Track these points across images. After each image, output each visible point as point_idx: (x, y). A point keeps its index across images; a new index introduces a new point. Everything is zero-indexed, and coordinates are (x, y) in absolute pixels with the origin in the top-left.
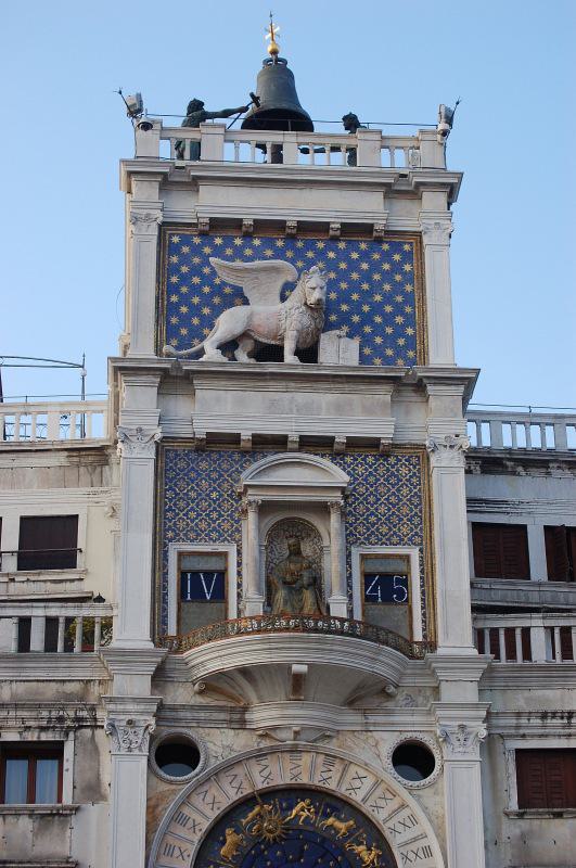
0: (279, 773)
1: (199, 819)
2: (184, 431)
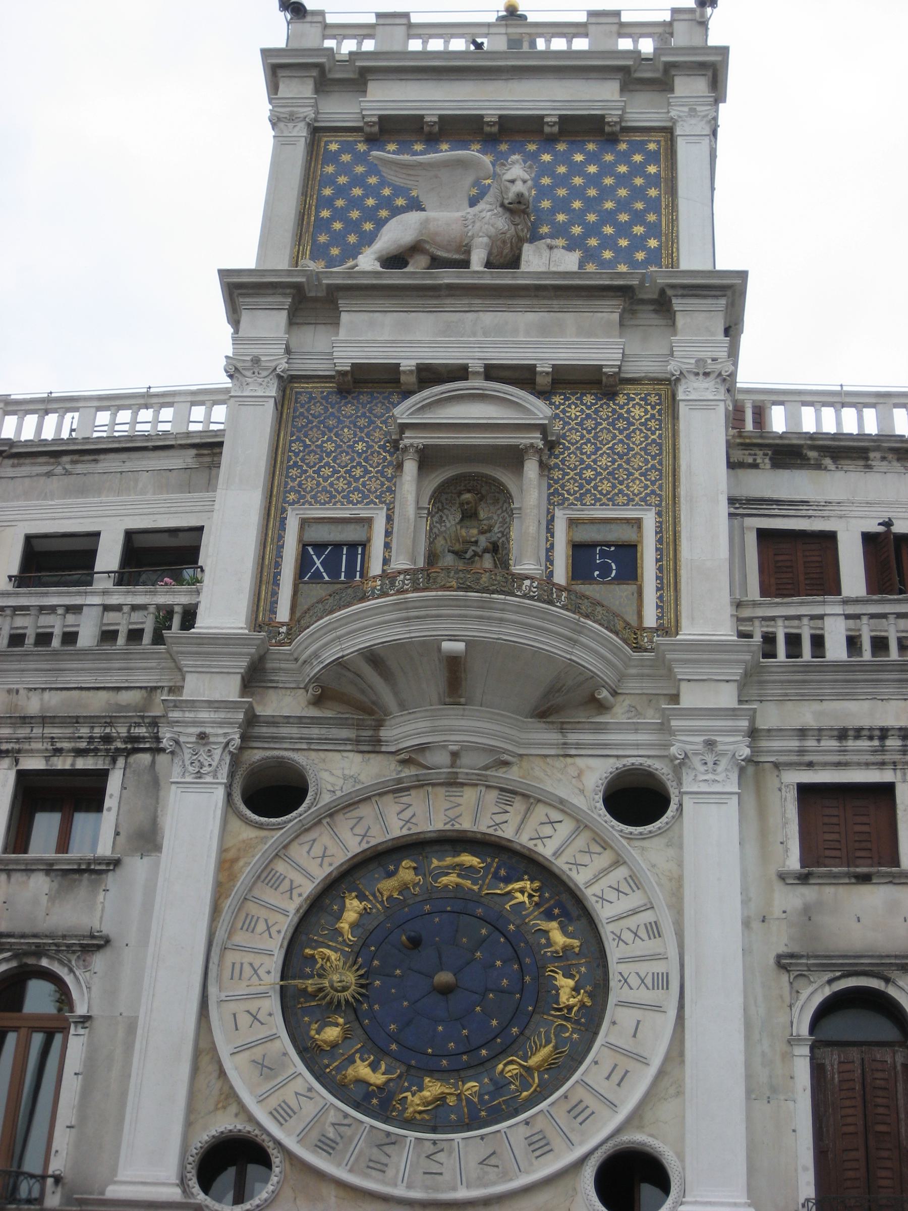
0: (430, 815)
1: (298, 879)
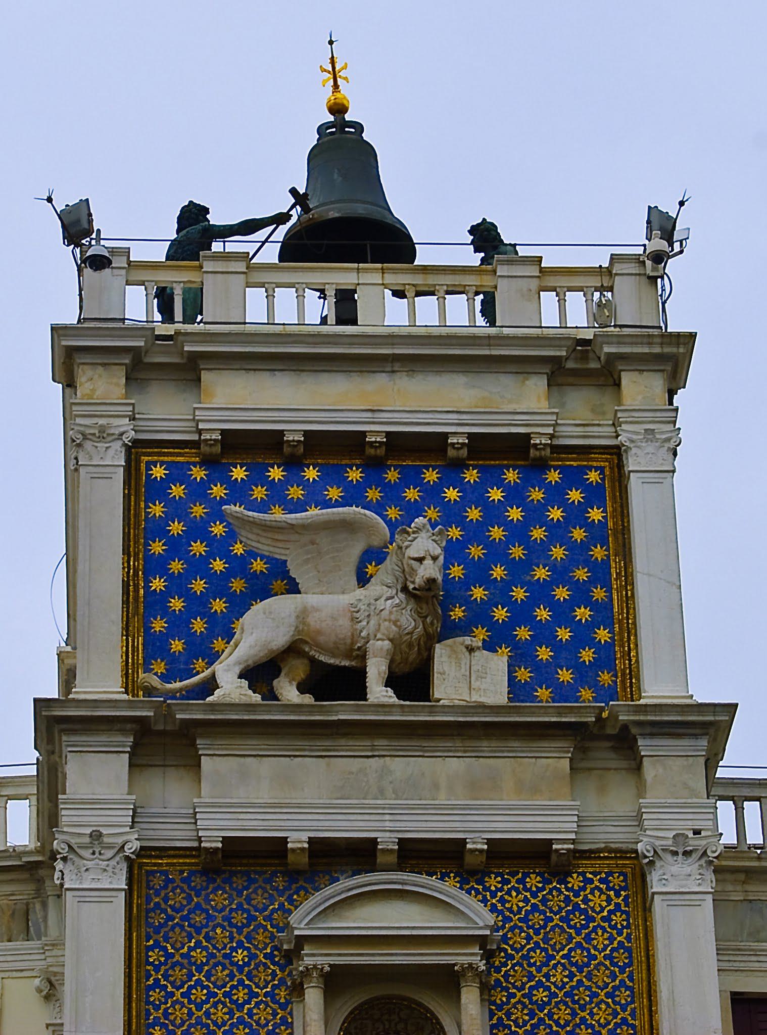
2: (178, 836)
